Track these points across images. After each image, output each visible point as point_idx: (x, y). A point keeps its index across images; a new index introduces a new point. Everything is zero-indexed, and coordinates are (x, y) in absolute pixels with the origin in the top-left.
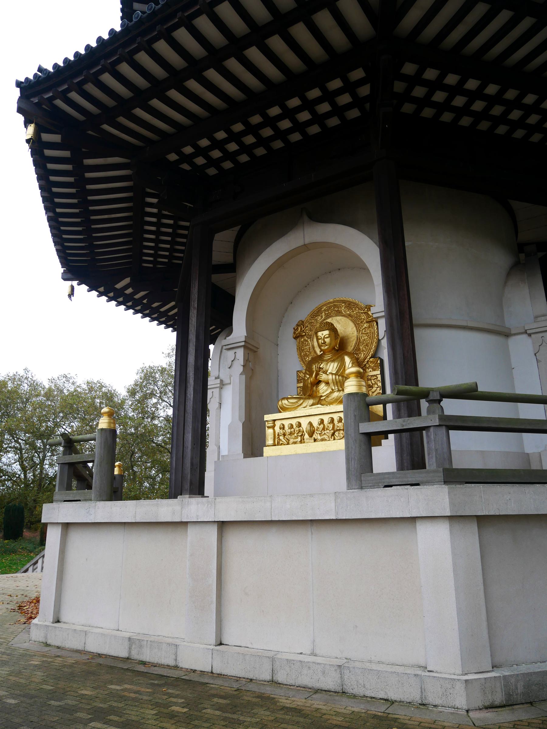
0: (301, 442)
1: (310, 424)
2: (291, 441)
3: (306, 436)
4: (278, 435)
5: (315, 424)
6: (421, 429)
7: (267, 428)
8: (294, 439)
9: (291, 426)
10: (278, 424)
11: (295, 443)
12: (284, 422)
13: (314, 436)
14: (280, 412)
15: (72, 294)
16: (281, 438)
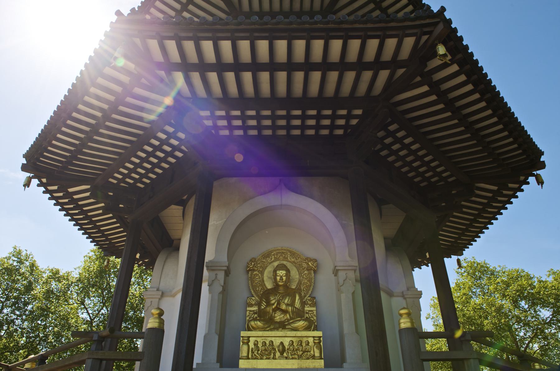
0: (274, 358)
1: (282, 343)
2: (265, 357)
3: (278, 354)
4: (252, 350)
5: (286, 344)
6: (462, 360)
7: (241, 343)
8: (267, 355)
9: (264, 344)
10: (252, 340)
11: (269, 359)
12: (259, 339)
13: (285, 354)
14: (251, 331)
15: (27, 184)
16: (256, 353)
